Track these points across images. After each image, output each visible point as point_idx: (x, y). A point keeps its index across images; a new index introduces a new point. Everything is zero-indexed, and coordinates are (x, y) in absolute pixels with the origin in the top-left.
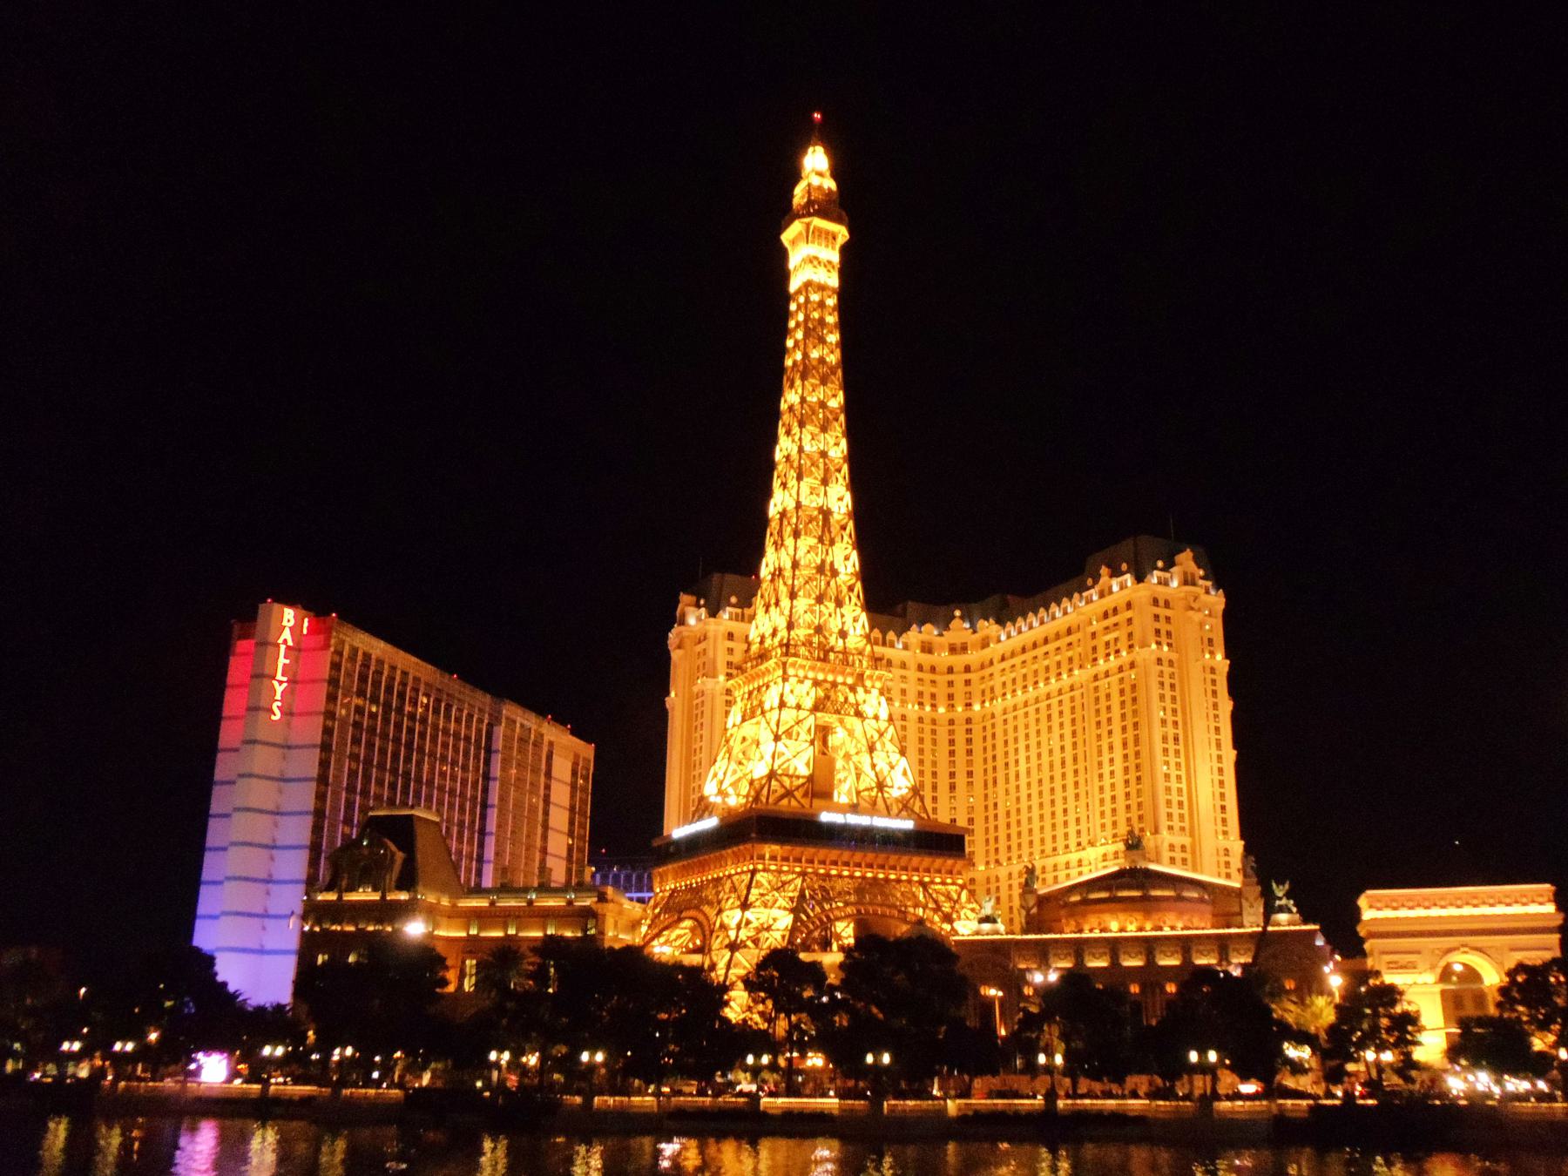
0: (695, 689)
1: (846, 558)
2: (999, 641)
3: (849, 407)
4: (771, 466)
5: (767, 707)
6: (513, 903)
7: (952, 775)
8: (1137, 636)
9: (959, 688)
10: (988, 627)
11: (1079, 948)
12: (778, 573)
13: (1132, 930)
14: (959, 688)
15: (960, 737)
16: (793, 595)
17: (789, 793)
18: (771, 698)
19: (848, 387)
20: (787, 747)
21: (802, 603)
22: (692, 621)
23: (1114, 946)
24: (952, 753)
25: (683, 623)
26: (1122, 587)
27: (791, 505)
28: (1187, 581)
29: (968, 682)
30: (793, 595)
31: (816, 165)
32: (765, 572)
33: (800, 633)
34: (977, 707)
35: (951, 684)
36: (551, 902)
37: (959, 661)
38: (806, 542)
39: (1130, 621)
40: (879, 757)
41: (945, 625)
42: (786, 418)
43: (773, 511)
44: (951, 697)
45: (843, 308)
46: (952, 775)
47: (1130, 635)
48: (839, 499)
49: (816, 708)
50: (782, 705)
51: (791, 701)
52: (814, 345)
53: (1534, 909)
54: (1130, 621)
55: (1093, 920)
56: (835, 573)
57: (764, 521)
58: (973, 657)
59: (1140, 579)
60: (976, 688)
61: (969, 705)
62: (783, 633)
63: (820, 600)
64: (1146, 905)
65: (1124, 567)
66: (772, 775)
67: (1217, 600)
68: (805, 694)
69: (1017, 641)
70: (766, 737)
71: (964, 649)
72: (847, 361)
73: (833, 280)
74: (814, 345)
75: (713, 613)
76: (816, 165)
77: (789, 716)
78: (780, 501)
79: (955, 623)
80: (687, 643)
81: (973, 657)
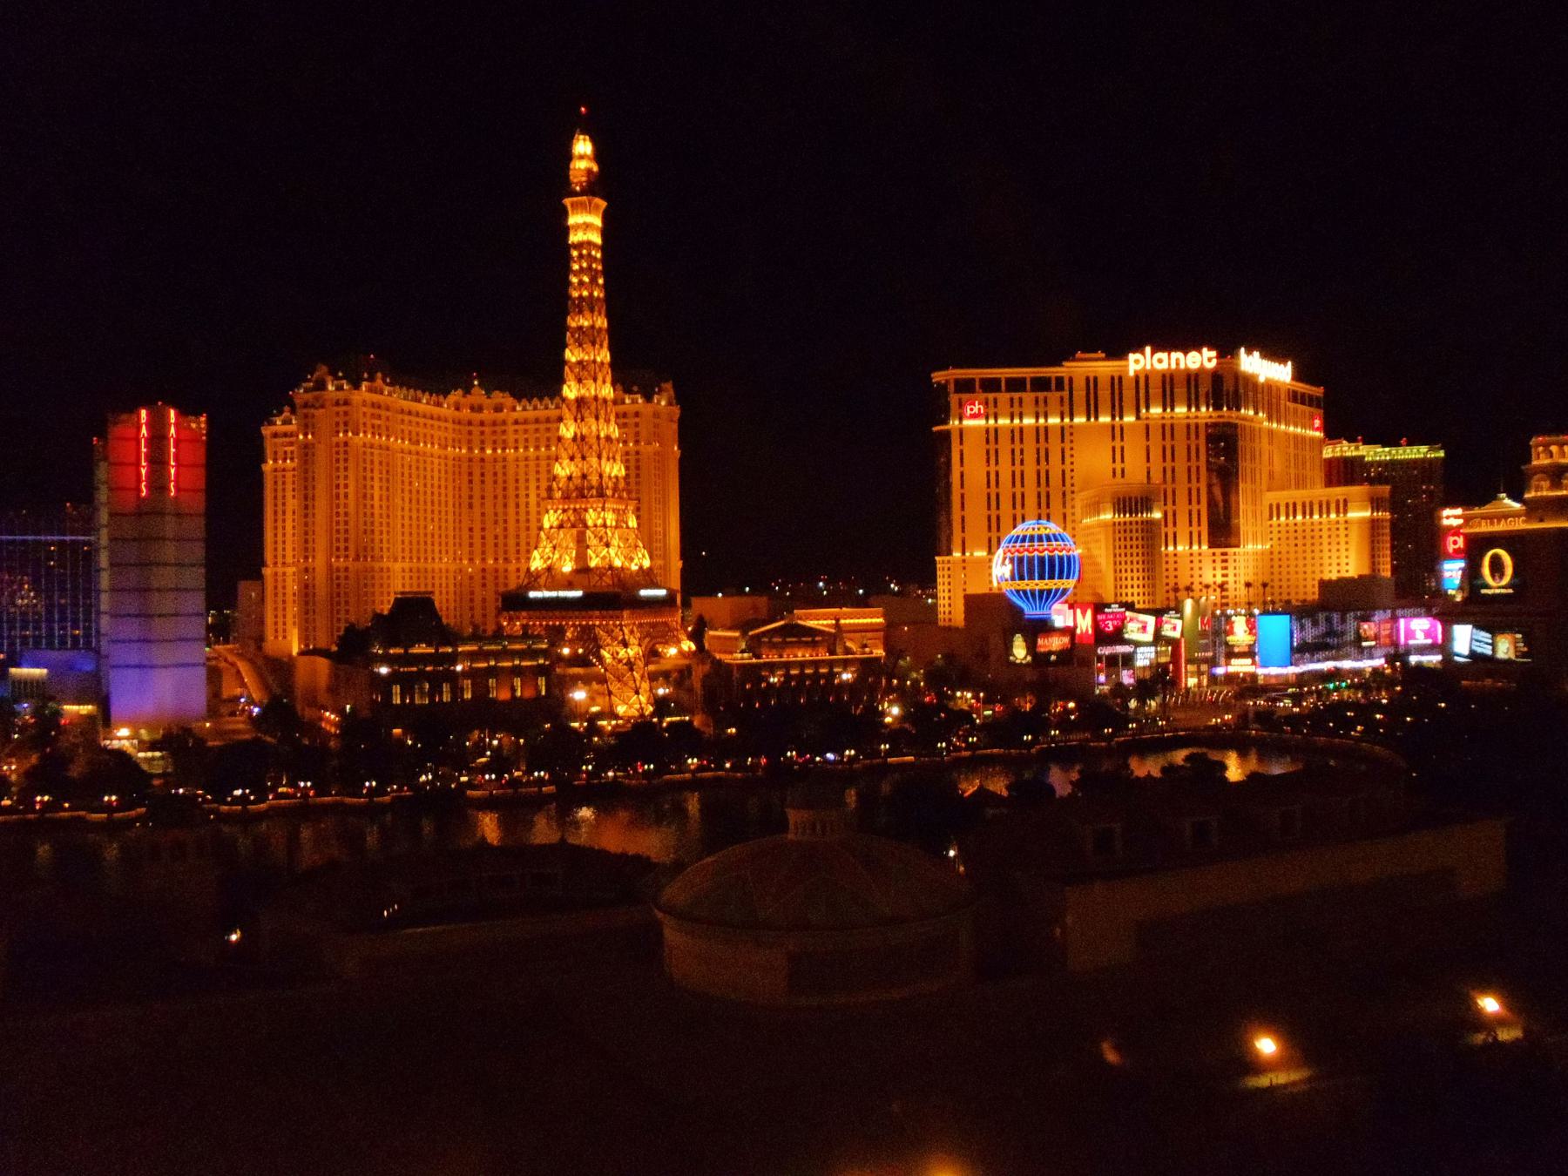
0: (335, 440)
2: (514, 409)
3: (612, 330)
5: (590, 523)
6: (493, 647)
7: (471, 497)
8: (644, 434)
9: (476, 438)
10: (509, 401)
11: (787, 666)
13: (808, 657)
14: (476, 438)
15: (477, 473)
19: (609, 317)
22: (331, 388)
23: (802, 665)
24: (470, 482)
25: (321, 386)
26: (634, 402)
28: (670, 404)
29: (482, 433)
31: (583, 146)
34: (489, 452)
35: (470, 433)
36: (517, 647)
37: (477, 417)
39: (637, 425)
41: (468, 390)
44: (469, 442)
45: (604, 261)
46: (471, 497)
47: (637, 434)
50: (605, 526)
53: (874, 620)
54: (637, 425)
55: (788, 651)
58: (487, 415)
59: (648, 399)
60: (489, 438)
61: (482, 449)
64: (814, 645)
65: (635, 389)
67: (676, 410)
69: (531, 414)
71: (480, 409)
72: (609, 299)
73: (597, 239)
74: (584, 283)
75: (357, 386)
76: (583, 146)
79: (476, 390)
80: (328, 404)
81: (487, 415)
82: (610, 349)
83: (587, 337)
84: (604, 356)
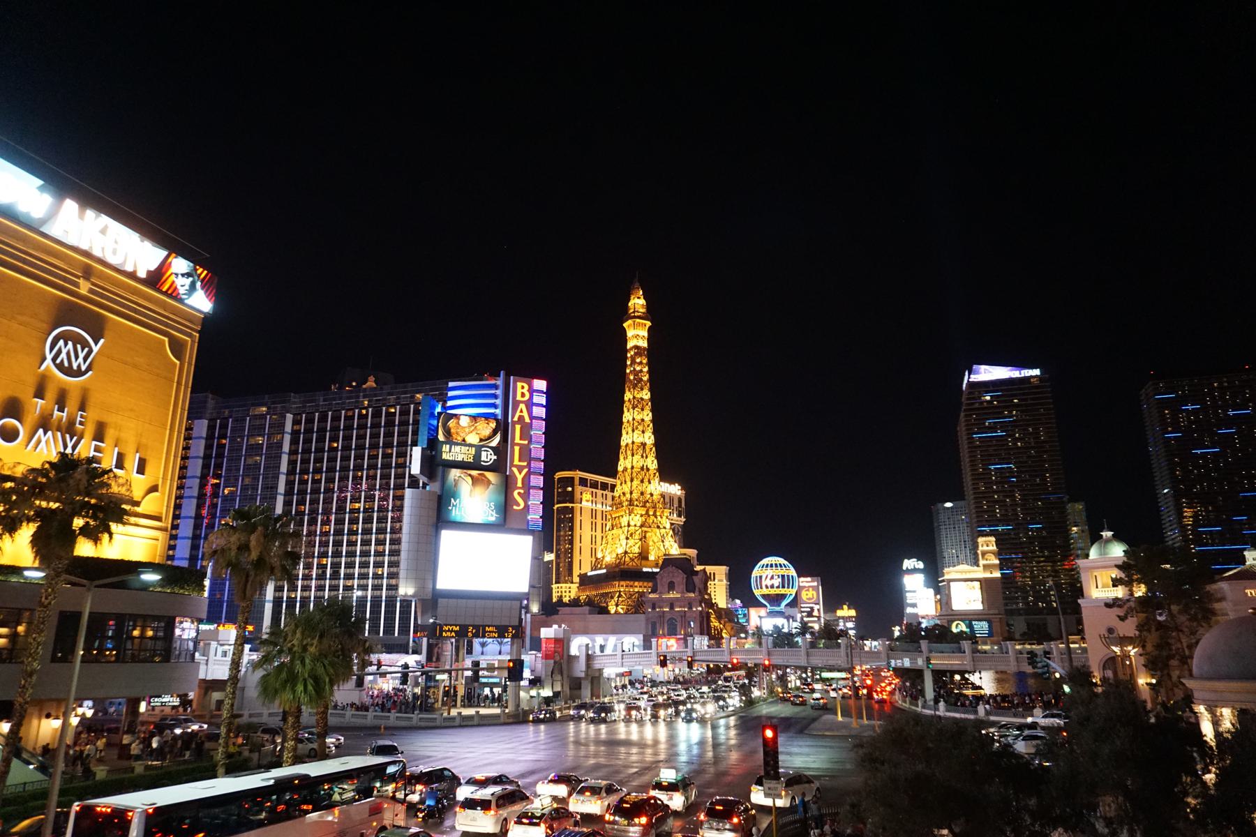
1: (652, 463)
4: (622, 423)
12: (625, 469)
16: (632, 480)
17: (632, 560)
18: (624, 521)
20: (631, 542)
21: (636, 482)
27: (630, 441)
30: (632, 480)
32: (620, 469)
33: (635, 496)
38: (637, 457)
40: (667, 544)
42: (627, 404)
43: (623, 443)
48: (649, 438)
49: (642, 526)
51: (632, 523)
52: (639, 368)
56: (648, 470)
57: (619, 446)
62: (628, 496)
63: (642, 481)
66: (626, 552)
68: (637, 520)
70: (623, 537)
77: (632, 529)
78: (626, 439)
82: (652, 410)
83: (638, 403)
84: (647, 416)
